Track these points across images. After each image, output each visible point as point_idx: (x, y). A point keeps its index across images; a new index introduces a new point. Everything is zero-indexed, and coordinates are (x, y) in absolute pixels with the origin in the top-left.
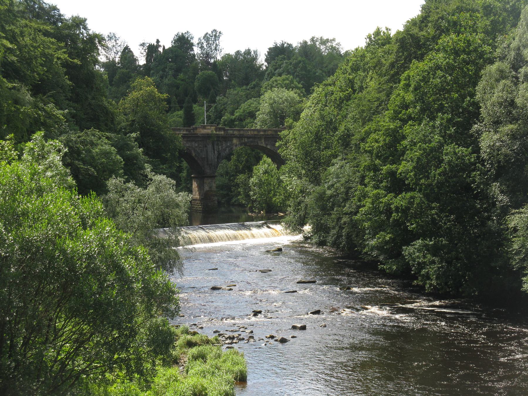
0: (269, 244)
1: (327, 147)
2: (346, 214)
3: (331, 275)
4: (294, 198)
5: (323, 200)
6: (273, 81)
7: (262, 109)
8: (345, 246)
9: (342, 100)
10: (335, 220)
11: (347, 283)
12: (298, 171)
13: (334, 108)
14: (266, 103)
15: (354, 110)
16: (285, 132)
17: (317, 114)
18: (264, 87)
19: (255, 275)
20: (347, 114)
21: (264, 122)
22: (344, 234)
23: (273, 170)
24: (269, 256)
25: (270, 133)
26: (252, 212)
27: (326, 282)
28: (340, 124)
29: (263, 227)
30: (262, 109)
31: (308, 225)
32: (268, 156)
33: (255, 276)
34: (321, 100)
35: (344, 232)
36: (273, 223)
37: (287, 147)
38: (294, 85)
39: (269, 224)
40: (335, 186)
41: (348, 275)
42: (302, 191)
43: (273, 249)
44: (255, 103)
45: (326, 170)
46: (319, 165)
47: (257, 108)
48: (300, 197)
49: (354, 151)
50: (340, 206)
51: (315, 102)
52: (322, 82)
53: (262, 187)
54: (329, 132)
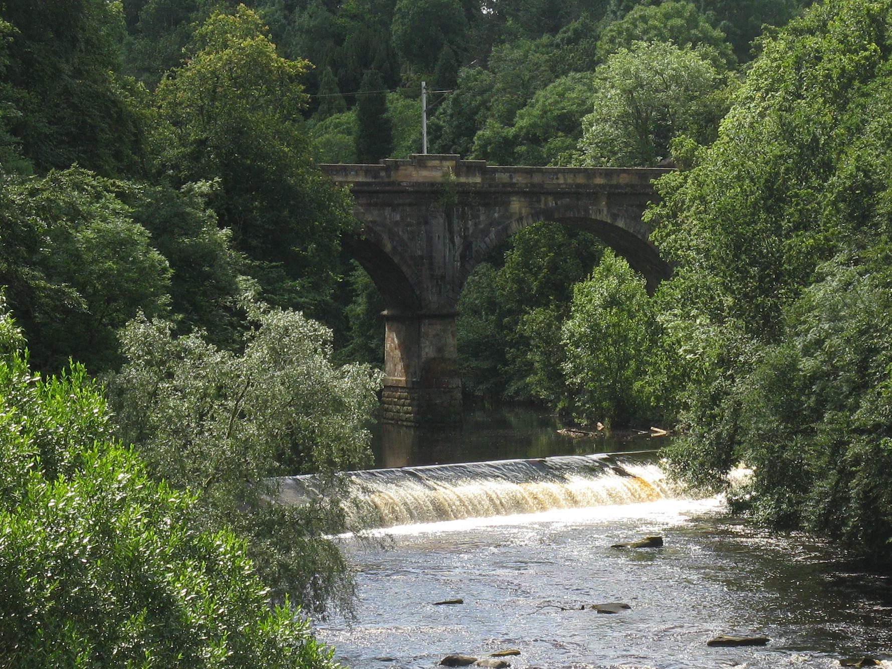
0: (621, 526)
1: (803, 225)
2: (860, 431)
3: (813, 619)
4: (698, 382)
5: (789, 386)
6: (635, 20)
7: (601, 106)
8: (859, 531)
9: (847, 79)
10: (828, 451)
11: (863, 644)
12: (712, 298)
13: (825, 102)
14: (613, 87)
15: (885, 111)
16: (671, 178)
17: (770, 123)
18: (605, 39)
19: (580, 620)
20: (864, 122)
21: (606, 145)
22: (853, 493)
23: (634, 296)
24: (622, 560)
25: (623, 179)
26: (570, 424)
27: (798, 640)
28: (842, 151)
29: (604, 472)
30: (601, 106)
31: (742, 465)
32: (620, 252)
33: (580, 624)
34: (781, 80)
35: (855, 488)
36: (642, 459)
37: (676, 224)
38: (701, 32)
39: (622, 462)
40: (827, 343)
41: (868, 621)
42: (723, 362)
43: (635, 540)
44: (579, 87)
45: (797, 294)
46: (777, 280)
47: (583, 102)
48: (717, 378)
49: (884, 237)
50: (841, 407)
51: (764, 83)
52: (785, 23)
53: (600, 349)
54: (807, 179)
